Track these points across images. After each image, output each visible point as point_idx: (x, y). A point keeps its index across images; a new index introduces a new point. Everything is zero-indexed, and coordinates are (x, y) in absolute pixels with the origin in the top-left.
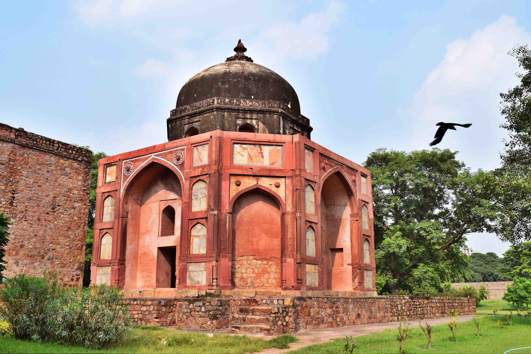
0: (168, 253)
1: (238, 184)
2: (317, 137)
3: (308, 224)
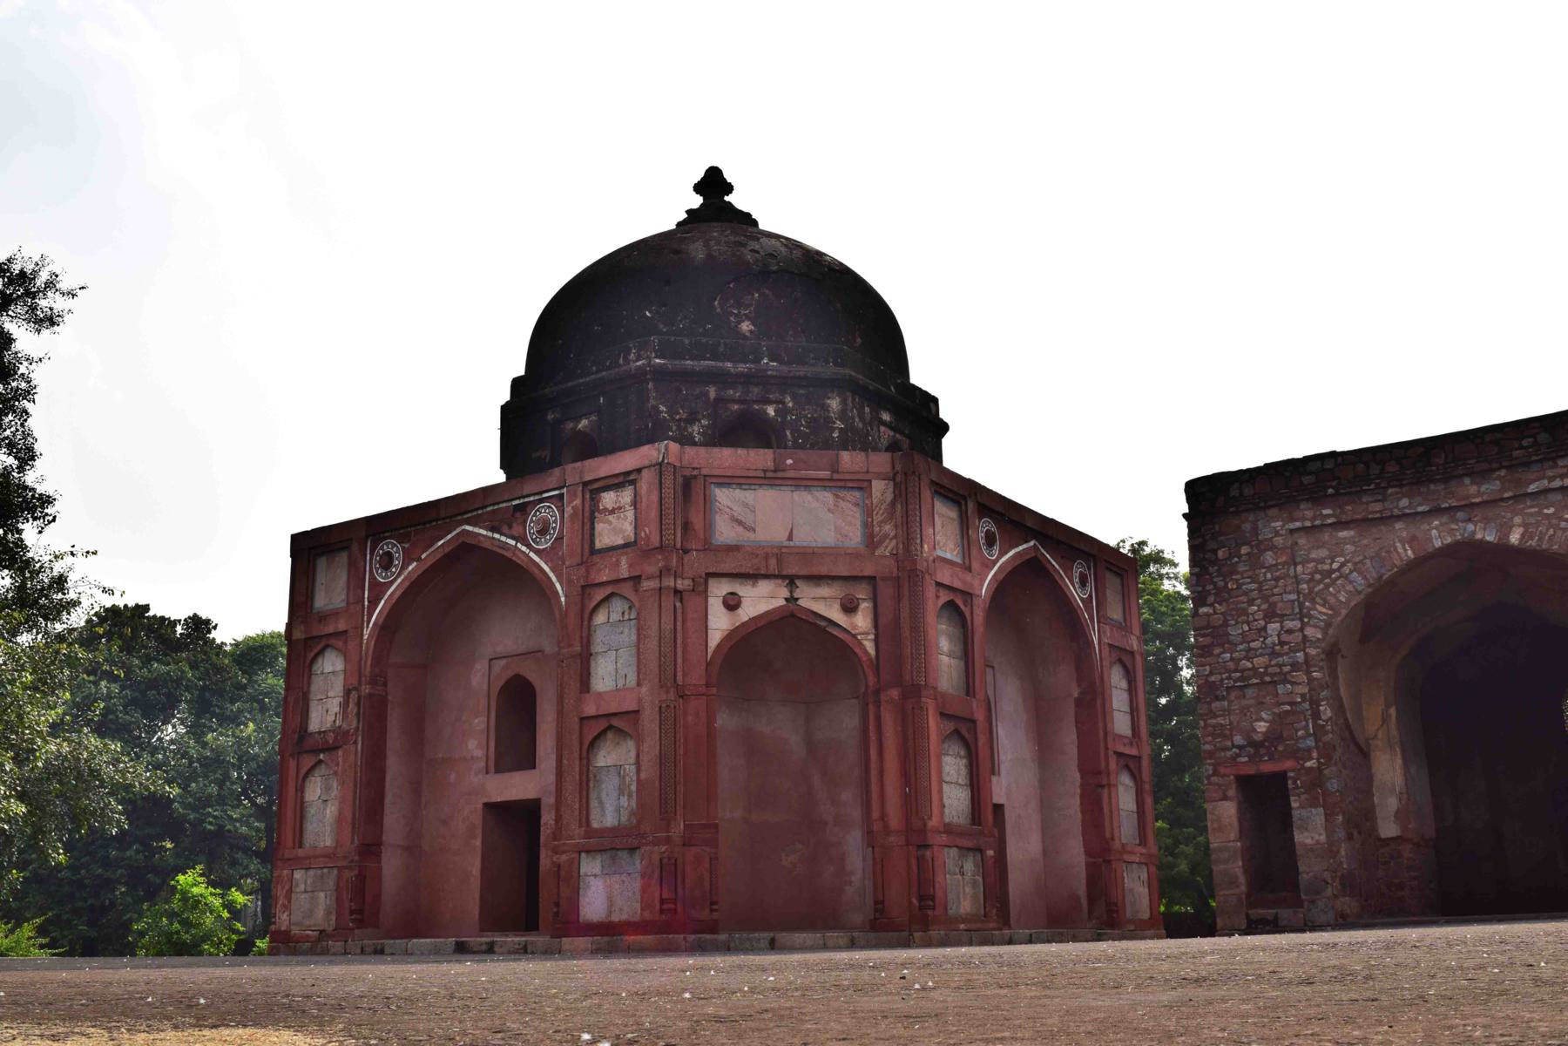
0: (516, 823)
1: (732, 603)
2: (957, 456)
3: (951, 726)
